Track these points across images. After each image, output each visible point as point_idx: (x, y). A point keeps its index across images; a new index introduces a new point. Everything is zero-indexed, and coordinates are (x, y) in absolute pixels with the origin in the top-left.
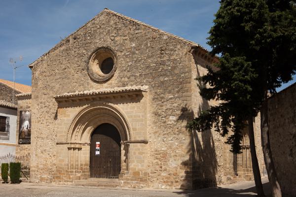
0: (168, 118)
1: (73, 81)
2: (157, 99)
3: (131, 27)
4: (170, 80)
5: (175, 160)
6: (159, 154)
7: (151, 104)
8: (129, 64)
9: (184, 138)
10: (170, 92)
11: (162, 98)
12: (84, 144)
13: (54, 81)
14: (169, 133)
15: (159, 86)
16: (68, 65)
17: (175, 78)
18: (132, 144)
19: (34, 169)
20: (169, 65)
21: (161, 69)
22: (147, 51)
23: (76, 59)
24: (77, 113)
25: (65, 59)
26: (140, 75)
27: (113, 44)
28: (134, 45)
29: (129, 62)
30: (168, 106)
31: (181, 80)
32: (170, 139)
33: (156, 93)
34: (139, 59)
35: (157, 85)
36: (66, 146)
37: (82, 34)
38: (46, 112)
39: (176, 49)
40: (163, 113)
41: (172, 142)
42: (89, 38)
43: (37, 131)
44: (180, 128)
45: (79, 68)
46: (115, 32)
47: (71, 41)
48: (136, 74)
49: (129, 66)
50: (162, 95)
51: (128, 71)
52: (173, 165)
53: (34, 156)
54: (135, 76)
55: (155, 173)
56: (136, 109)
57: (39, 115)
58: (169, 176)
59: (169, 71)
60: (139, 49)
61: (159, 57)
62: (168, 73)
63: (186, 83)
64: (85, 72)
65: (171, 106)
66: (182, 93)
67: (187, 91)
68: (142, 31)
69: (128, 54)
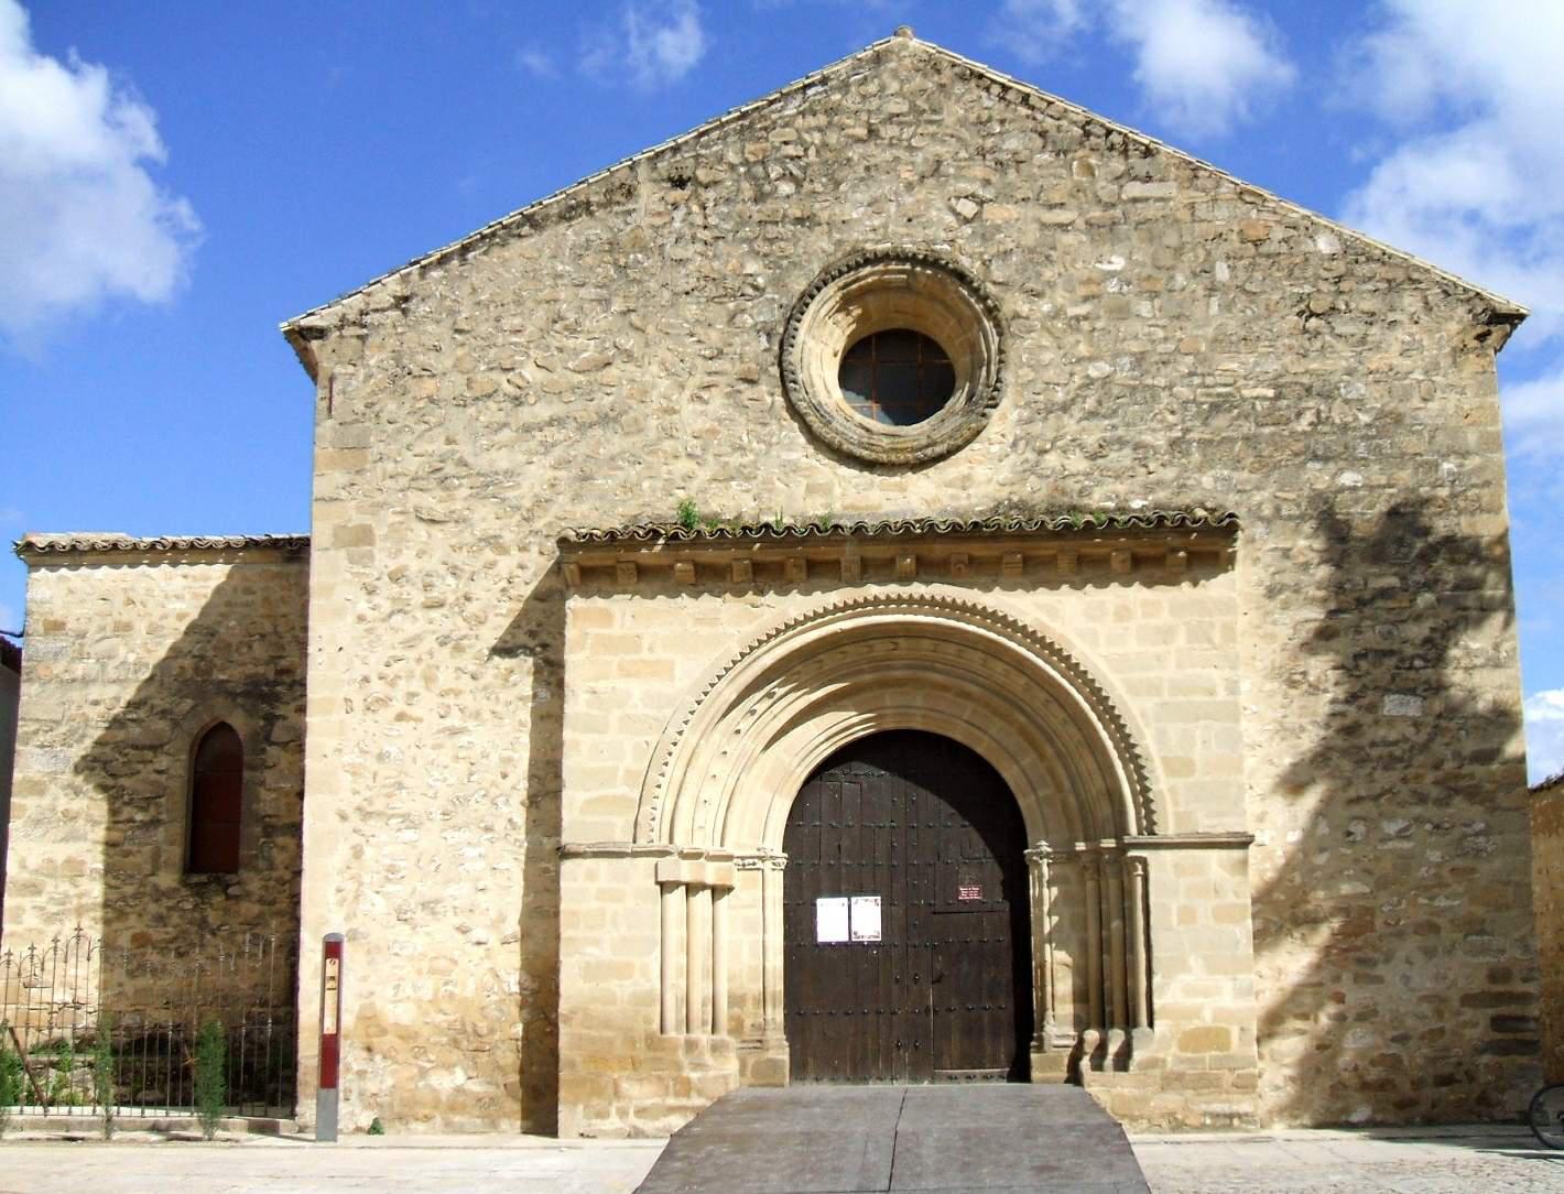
0: (1372, 708)
1: (668, 445)
5: (1429, 953)
9: (1480, 826)
12: (747, 864)
13: (506, 434)
16: (630, 342)
22: (1214, 309)
25: (605, 302)
26: (1173, 443)
27: (977, 247)
28: (1118, 263)
29: (1091, 359)
32: (1391, 828)
33: (1286, 553)
34: (1161, 348)
41: (1407, 845)
42: (786, 188)
44: (1449, 766)
45: (715, 365)
48: (1148, 438)
49: (1089, 382)
51: (1092, 415)
52: (1416, 981)
56: (1181, 640)
58: (1394, 1049)
59: (1365, 438)
61: (1290, 348)
62: (1361, 450)
63: (1472, 513)
64: (767, 393)
65: (1388, 636)
68: (1169, 189)
69: (1083, 310)
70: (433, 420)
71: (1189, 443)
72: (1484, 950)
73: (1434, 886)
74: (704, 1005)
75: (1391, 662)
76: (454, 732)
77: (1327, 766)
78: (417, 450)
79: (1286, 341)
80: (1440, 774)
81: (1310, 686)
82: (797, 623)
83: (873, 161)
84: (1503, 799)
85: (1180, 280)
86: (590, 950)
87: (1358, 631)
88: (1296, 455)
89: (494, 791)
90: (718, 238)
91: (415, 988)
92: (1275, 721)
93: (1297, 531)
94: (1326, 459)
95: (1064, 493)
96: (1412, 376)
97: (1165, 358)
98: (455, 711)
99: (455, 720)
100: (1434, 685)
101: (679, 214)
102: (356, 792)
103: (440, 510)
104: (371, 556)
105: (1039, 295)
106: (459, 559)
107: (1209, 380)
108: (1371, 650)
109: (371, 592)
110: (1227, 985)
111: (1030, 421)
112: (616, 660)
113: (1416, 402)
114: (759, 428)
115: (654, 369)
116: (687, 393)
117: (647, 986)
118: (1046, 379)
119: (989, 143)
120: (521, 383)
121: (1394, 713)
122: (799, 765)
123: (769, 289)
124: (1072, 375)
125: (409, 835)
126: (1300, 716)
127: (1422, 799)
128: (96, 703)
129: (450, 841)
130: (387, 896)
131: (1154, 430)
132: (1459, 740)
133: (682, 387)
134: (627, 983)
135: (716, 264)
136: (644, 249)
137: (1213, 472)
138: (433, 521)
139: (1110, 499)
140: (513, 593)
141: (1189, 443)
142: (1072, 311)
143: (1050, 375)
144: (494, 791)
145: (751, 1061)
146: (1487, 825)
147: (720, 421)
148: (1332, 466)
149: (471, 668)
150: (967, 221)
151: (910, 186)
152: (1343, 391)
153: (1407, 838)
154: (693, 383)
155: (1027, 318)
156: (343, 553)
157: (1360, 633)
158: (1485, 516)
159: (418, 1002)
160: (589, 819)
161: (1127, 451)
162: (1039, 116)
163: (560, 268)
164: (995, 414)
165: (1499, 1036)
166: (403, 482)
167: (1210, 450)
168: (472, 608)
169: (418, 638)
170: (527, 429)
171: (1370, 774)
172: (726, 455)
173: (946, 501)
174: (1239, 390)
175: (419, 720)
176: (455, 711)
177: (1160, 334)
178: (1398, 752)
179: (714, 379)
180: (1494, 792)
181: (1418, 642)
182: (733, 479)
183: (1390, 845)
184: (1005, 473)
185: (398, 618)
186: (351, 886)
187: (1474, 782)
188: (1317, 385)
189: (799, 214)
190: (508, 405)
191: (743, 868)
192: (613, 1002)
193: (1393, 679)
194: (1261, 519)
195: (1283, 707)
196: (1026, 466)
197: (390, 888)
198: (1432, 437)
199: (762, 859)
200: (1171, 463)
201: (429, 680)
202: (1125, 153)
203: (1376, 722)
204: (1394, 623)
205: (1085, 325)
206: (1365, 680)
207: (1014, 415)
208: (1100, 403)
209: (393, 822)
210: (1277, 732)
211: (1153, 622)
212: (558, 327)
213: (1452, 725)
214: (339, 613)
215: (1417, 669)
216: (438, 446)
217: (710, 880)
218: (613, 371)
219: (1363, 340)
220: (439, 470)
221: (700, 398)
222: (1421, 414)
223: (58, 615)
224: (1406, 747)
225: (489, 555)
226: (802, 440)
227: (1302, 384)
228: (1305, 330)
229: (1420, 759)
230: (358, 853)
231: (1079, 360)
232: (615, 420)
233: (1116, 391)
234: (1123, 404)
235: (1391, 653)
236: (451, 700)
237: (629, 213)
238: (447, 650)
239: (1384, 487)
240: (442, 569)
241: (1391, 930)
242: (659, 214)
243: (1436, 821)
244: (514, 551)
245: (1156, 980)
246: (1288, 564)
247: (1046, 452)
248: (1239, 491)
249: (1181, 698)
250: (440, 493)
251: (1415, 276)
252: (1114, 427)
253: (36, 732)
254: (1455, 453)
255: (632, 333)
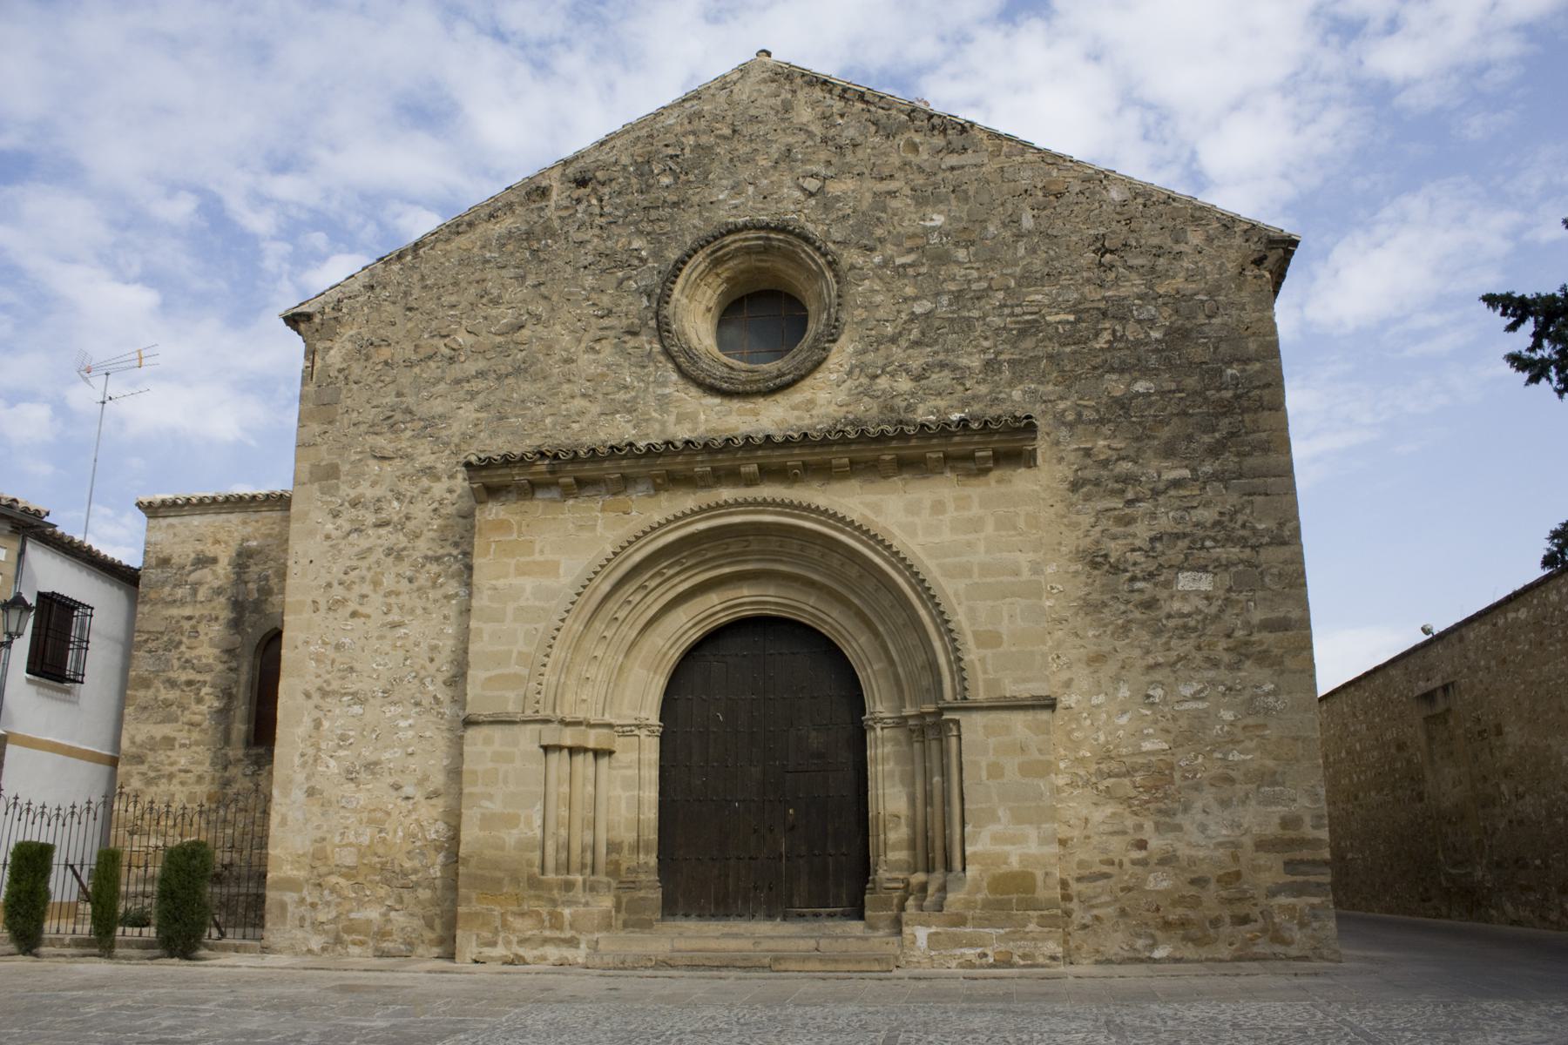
0: (1167, 584)
1: (566, 387)
2: (1097, 483)
3: (917, 139)
4: (1162, 393)
5: (1225, 803)
6: (1128, 774)
7: (1060, 507)
8: (918, 309)
9: (1269, 687)
10: (1169, 451)
11: (1127, 479)
12: (626, 731)
13: (442, 387)
14: (1180, 659)
15: (1102, 421)
16: (540, 308)
17: (1192, 382)
18: (978, 719)
19: (288, 871)
20: (1152, 321)
21: (1106, 336)
22: (1021, 252)
23: (589, 281)
24: (609, 550)
25: (521, 279)
26: (988, 363)
28: (939, 220)
29: (916, 298)
30: (1165, 523)
31: (1228, 394)
32: (1187, 691)
34: (974, 286)
35: (1089, 414)
36: (527, 739)
37: (625, 160)
38: (389, 552)
39: (1182, 247)
40: (1138, 556)
41: (1201, 705)
42: (666, 180)
43: (319, 659)
44: (1239, 634)
45: (606, 322)
46: (823, 155)
47: (554, 196)
48: (964, 361)
49: (913, 317)
50: (1126, 466)
51: (916, 344)
53: (298, 795)
54: (955, 368)
55: (1106, 876)
56: (990, 529)
57: (337, 570)
59: (1156, 351)
60: (973, 243)
61: (1088, 280)
63: (1256, 411)
66: (1238, 454)
67: (1265, 447)
70: (388, 379)
71: (1000, 363)
72: (1273, 800)
73: (1227, 742)
74: (583, 851)
75: (1187, 542)
76: (395, 626)
77: (1127, 637)
78: (375, 403)
79: (1085, 274)
80: (1231, 643)
81: (1111, 566)
82: (661, 525)
83: (736, 153)
84: (1289, 663)
85: (992, 229)
86: (486, 804)
87: (1153, 516)
88: (1095, 368)
89: (423, 673)
90: (611, 223)
91: (357, 835)
92: (1079, 598)
93: (1097, 433)
94: (1122, 371)
95: (892, 410)
96: (1196, 298)
97: (979, 294)
98: (395, 610)
99: (395, 617)
100: (1224, 562)
101: (581, 208)
102: (318, 676)
103: (389, 449)
104: (338, 488)
105: (872, 250)
106: (404, 486)
107: (1018, 310)
108: (1166, 533)
109: (336, 515)
110: (1032, 832)
111: (864, 352)
112: (513, 562)
113: (1202, 319)
114: (639, 370)
115: (558, 327)
116: (583, 345)
117: (530, 834)
118: (878, 316)
119: (832, 132)
120: (455, 346)
121: (1187, 588)
122: (671, 647)
123: (650, 260)
124: (899, 312)
125: (357, 709)
126: (1102, 593)
127: (1215, 664)
128: (190, 618)
129: (388, 715)
130: (338, 759)
131: (971, 354)
132: (1248, 611)
133: (579, 341)
134: (515, 831)
135: (609, 243)
136: (553, 235)
137: (1021, 387)
138: (384, 458)
139: (933, 414)
140: (443, 511)
141: (1000, 363)
142: (899, 261)
143: (881, 313)
144: (423, 673)
145: (624, 900)
146: (1277, 686)
147: (608, 366)
148: (1127, 376)
149: (408, 573)
150: (811, 195)
151: (765, 172)
152: (1135, 313)
153: (1202, 699)
154: (587, 337)
155: (862, 269)
156: (316, 486)
157: (1156, 518)
158: (1266, 413)
159: (359, 847)
160: (488, 693)
161: (946, 372)
162: (873, 109)
163: (488, 255)
164: (835, 348)
165: (1290, 878)
166: (363, 428)
167: (1019, 368)
168: (410, 525)
169: (370, 549)
170: (458, 382)
171: (1167, 643)
172: (613, 393)
173: (792, 421)
174: (1043, 317)
175: (368, 616)
176: (395, 610)
177: (975, 274)
178: (1192, 623)
179: (605, 333)
180: (1282, 656)
181: (1208, 525)
182: (618, 412)
183: (1186, 706)
184: (842, 397)
185: (355, 535)
186: (311, 751)
187: (1264, 647)
188: (1111, 311)
189: (675, 199)
190: (445, 364)
191: (623, 734)
192: (502, 848)
193: (1186, 558)
194: (1064, 424)
195: (1086, 585)
196: (860, 389)
197: (342, 753)
198: (1216, 348)
199: (639, 727)
200: (985, 380)
201: (376, 584)
202: (944, 131)
203: (1172, 597)
204: (1187, 509)
205: (911, 271)
206: (1161, 560)
207: (850, 349)
208: (923, 334)
209: (345, 699)
210: (1081, 607)
211: (966, 514)
212: (484, 300)
213: (1242, 597)
214: (311, 533)
215: (1208, 549)
216: (390, 399)
217: (591, 745)
218: (526, 332)
219: (1153, 269)
220: (389, 418)
221: (593, 349)
222: (1206, 329)
223: (166, 554)
224: (1199, 618)
225: (425, 482)
226: (674, 377)
227: (1098, 309)
228: (1100, 264)
229: (1211, 629)
230: (318, 724)
231: (906, 300)
232: (526, 370)
233: (937, 324)
234: (942, 334)
235: (1185, 535)
236: (392, 600)
237: (542, 209)
238: (390, 560)
239: (1174, 392)
240: (389, 495)
241: (1190, 782)
242: (567, 208)
243: (1229, 684)
244: (445, 479)
245: (968, 829)
246: (1089, 461)
247: (877, 376)
248: (1045, 402)
249: (989, 580)
250: (389, 435)
251: (1198, 214)
252: (936, 353)
253: (146, 641)
254: (1238, 360)
255: (542, 302)
